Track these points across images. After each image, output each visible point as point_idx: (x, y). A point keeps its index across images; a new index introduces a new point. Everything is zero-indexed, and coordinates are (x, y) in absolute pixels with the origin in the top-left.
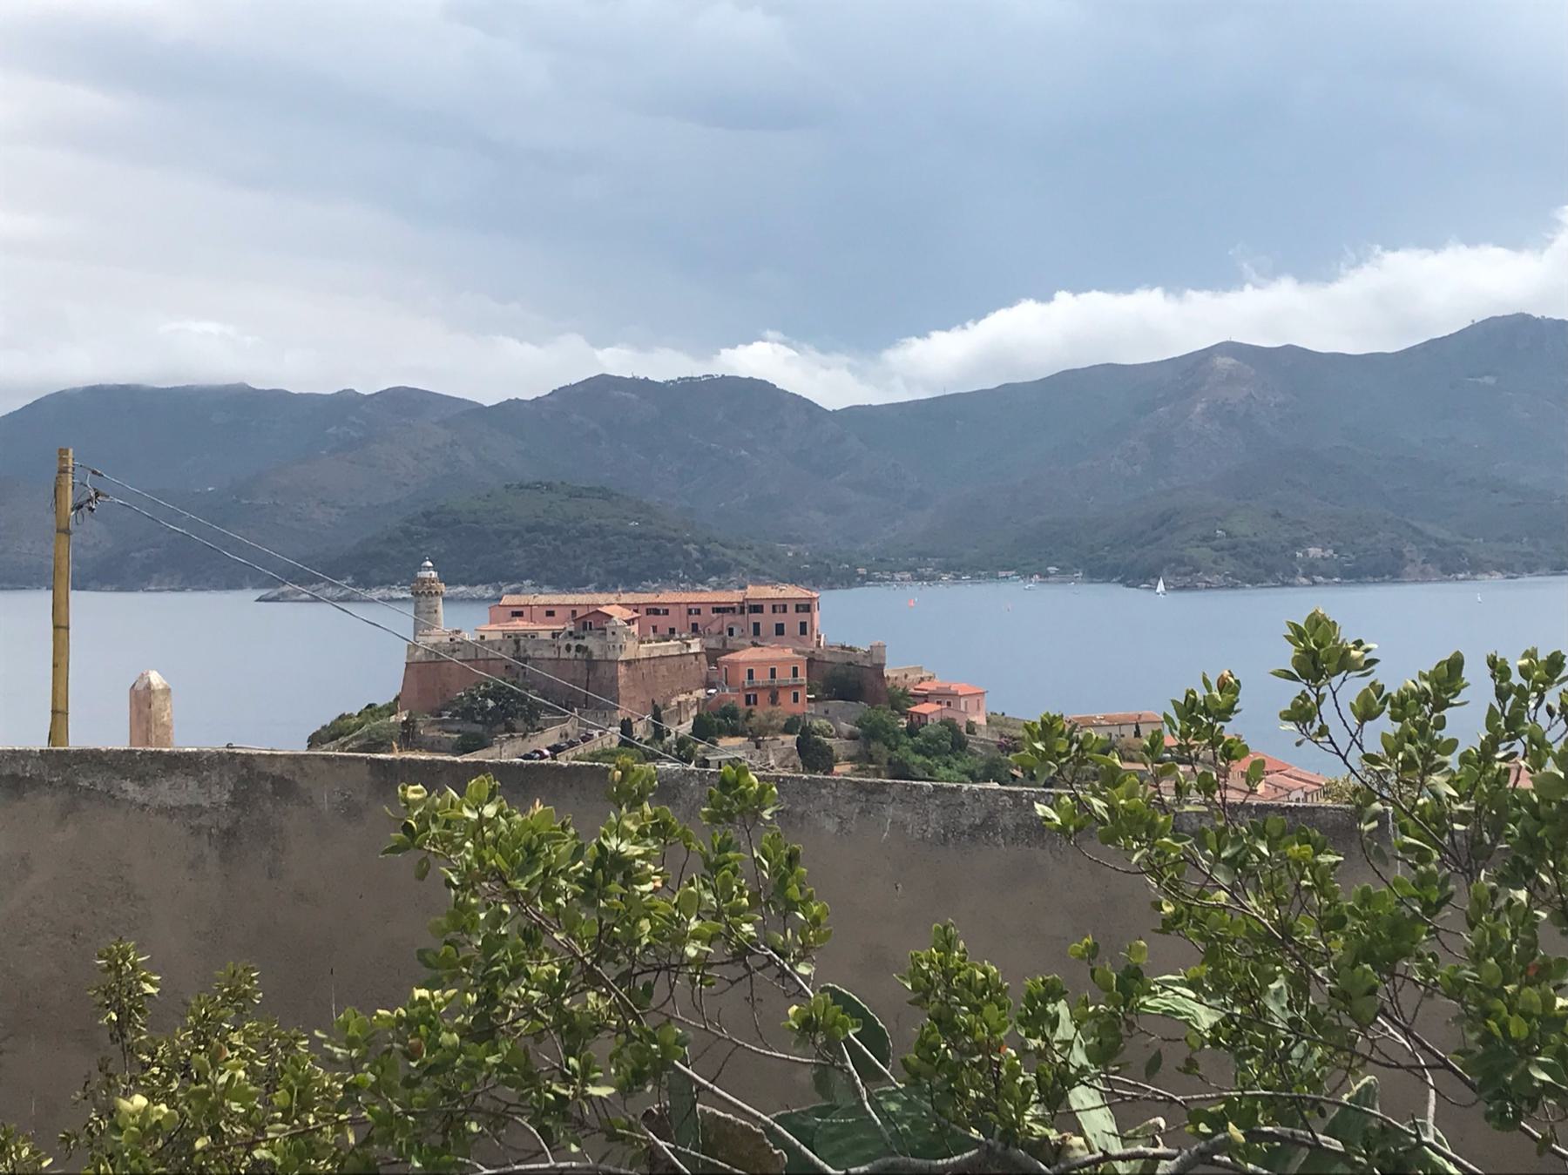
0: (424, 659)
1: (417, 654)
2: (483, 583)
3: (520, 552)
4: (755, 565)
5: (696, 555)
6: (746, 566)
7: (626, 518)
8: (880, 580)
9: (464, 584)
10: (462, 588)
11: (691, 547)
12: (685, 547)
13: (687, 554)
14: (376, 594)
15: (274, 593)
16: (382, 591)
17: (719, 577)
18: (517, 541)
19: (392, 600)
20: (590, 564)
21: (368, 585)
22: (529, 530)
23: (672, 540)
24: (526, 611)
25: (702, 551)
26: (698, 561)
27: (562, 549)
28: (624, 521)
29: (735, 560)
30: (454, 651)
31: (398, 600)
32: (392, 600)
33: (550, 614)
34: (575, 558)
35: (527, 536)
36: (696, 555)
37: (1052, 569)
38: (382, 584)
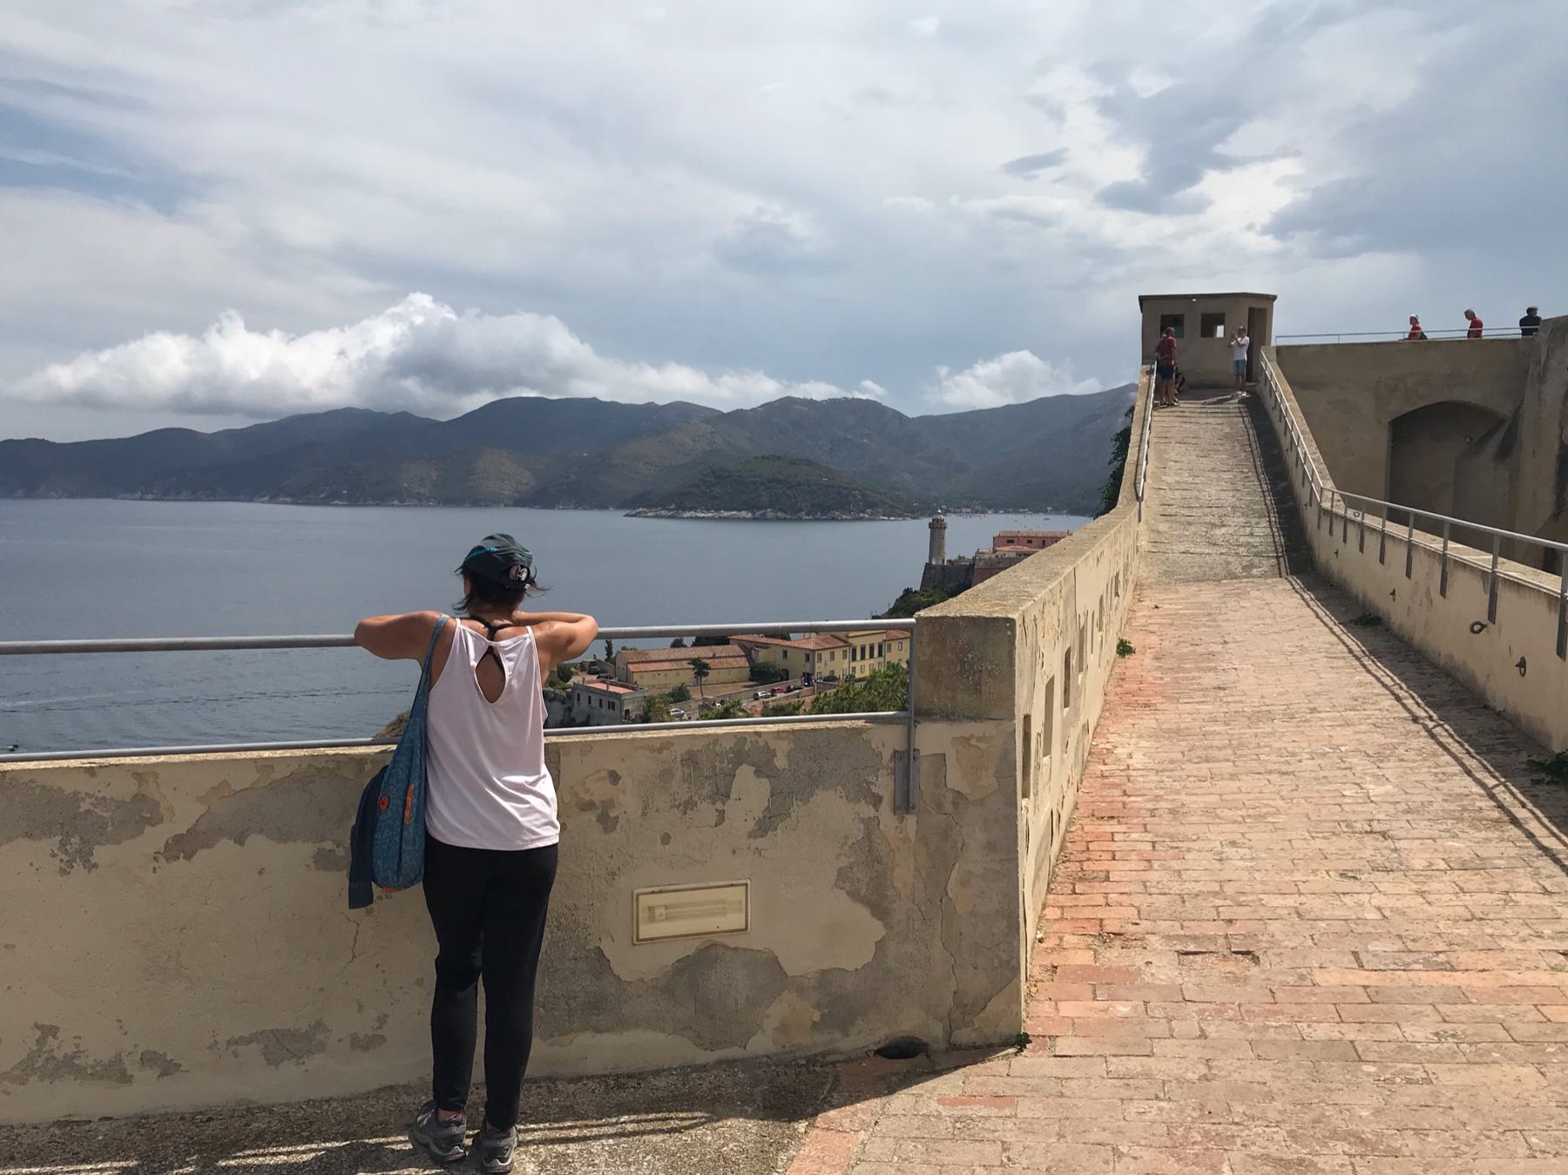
2: (745, 510)
3: (764, 493)
4: (890, 502)
5: (859, 497)
6: (886, 503)
8: (955, 513)
10: (734, 512)
11: (857, 492)
13: (855, 496)
14: (688, 514)
15: (634, 512)
16: (692, 512)
18: (763, 487)
19: (697, 518)
21: (684, 510)
22: (769, 482)
23: (846, 489)
24: (1016, 540)
25: (863, 495)
26: (860, 500)
27: (787, 492)
30: (999, 563)
32: (697, 518)
33: (1030, 542)
35: (768, 485)
36: (859, 497)
37: (1049, 508)
38: (690, 509)
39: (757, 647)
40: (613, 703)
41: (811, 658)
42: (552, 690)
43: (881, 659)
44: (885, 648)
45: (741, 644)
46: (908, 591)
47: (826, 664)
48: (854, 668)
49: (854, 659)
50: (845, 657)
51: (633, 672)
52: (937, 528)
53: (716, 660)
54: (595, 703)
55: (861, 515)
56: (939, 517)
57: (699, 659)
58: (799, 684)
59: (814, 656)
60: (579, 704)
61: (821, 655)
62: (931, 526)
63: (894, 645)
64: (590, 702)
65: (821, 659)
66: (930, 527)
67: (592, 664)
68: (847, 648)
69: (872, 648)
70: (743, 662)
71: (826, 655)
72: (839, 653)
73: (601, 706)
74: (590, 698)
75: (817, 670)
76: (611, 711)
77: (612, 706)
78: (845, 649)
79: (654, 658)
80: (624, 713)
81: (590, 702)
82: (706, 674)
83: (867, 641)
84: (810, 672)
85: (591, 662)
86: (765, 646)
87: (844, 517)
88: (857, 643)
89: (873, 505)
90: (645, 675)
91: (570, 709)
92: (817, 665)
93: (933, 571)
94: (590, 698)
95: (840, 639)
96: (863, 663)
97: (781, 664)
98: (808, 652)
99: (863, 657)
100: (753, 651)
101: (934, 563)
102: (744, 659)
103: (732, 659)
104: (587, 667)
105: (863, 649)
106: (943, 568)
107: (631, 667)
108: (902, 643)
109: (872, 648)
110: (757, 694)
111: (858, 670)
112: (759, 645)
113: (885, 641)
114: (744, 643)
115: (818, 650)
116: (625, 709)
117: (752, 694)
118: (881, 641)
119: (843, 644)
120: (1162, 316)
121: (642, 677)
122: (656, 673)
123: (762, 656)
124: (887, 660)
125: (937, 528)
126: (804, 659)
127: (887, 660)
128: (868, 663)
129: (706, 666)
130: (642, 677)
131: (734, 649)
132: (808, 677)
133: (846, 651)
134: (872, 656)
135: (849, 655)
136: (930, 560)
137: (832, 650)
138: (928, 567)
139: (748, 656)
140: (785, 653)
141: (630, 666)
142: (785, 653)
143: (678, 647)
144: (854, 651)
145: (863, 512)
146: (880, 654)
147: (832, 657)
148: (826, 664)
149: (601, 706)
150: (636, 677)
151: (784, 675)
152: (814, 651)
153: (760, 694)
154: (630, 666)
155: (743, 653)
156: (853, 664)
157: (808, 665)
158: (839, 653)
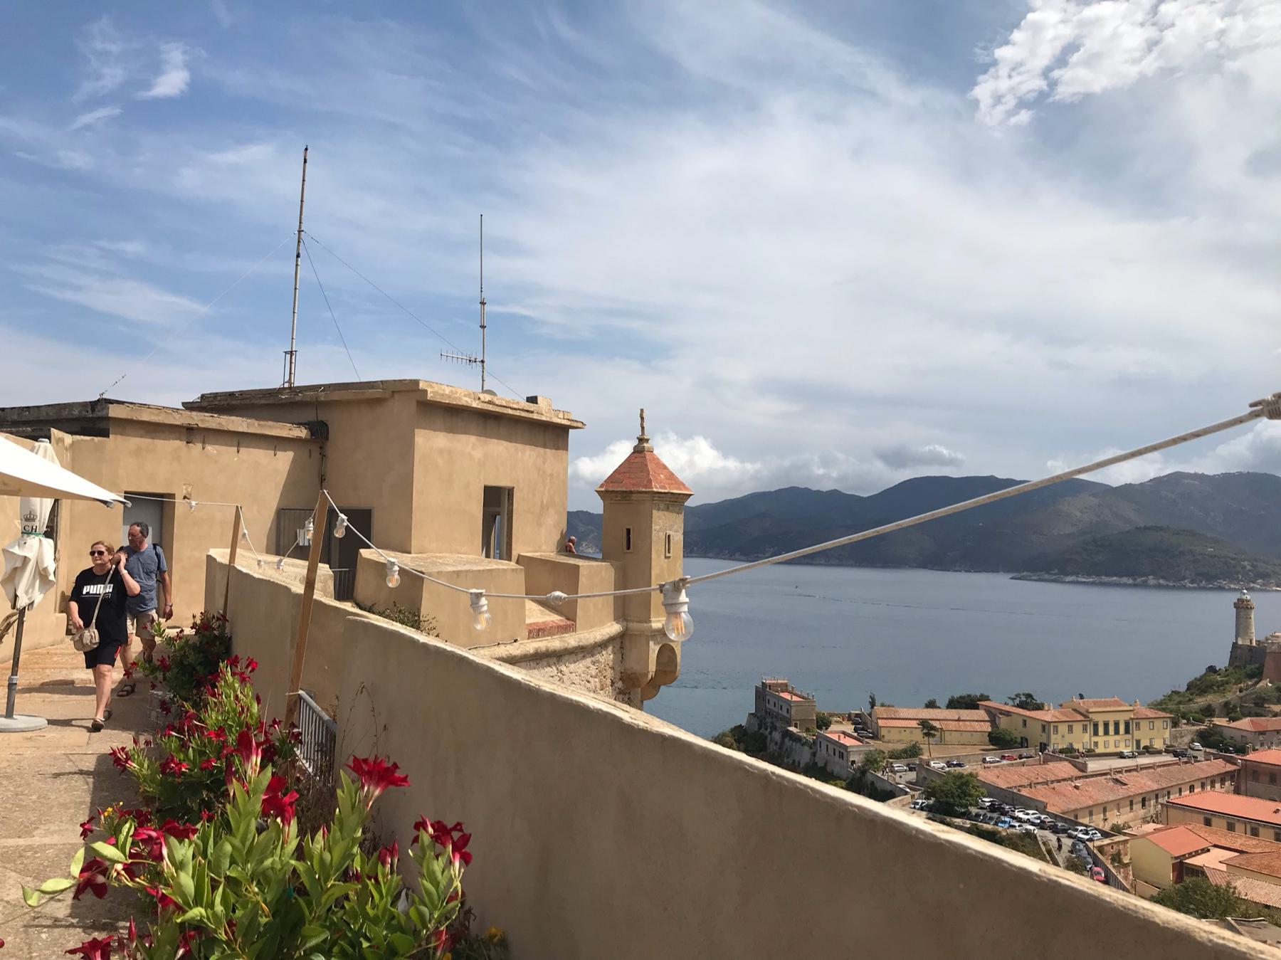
0: (1277, 651)
1: (1273, 647)
2: (1126, 576)
5: (1248, 567)
7: (1206, 546)
9: (1116, 575)
10: (1115, 578)
11: (1246, 563)
12: (1242, 563)
14: (1069, 579)
16: (1073, 577)
17: (1264, 580)
20: (1186, 569)
21: (1067, 575)
23: (1233, 559)
25: (1252, 566)
26: (1249, 570)
28: (1205, 548)
29: (1273, 571)
34: (1178, 566)
36: (1248, 567)
38: (1072, 574)
39: (1001, 714)
40: (843, 754)
41: (1046, 728)
42: (805, 735)
43: (1129, 736)
44: (1132, 726)
45: (989, 711)
46: (1212, 669)
47: (1063, 736)
48: (1096, 744)
49: (1096, 733)
51: (881, 727)
52: (1242, 608)
53: (961, 723)
54: (831, 752)
55: (1252, 585)
56: (1244, 597)
58: (1032, 752)
60: (821, 751)
61: (1057, 727)
62: (1236, 606)
63: (1144, 724)
64: (827, 750)
65: (1057, 731)
66: (1235, 607)
67: (857, 715)
68: (1088, 723)
69: (1117, 724)
70: (987, 727)
71: (1063, 728)
72: (1078, 728)
73: (834, 754)
74: (827, 746)
76: (841, 759)
77: (841, 756)
78: (1085, 723)
79: (902, 715)
80: (850, 764)
81: (827, 750)
82: (934, 736)
83: (1111, 718)
84: (1045, 741)
85: (857, 714)
86: (1008, 714)
87: (1232, 586)
88: (1100, 719)
89: (1264, 576)
90: (892, 730)
91: (814, 754)
92: (1053, 737)
93: (1239, 651)
94: (827, 746)
95: (1081, 714)
96: (1107, 738)
97: (1018, 734)
98: (1045, 723)
99: (1106, 733)
100: (997, 718)
101: (1240, 642)
102: (989, 724)
103: (977, 723)
104: (853, 717)
105: (1106, 725)
106: (1250, 648)
107: (881, 723)
108: (1153, 722)
109: (1117, 724)
110: (985, 759)
111: (1101, 745)
112: (1003, 712)
113: (1132, 719)
114: (993, 711)
115: (1053, 722)
116: (851, 759)
117: (981, 757)
118: (1127, 718)
119: (1082, 718)
121: (889, 732)
122: (903, 730)
123: (1003, 722)
124: (1135, 738)
125: (1242, 608)
126: (1040, 728)
127: (1135, 738)
128: (1112, 738)
129: (934, 728)
130: (889, 732)
131: (981, 714)
132: (1043, 747)
133: (1086, 725)
134: (1117, 732)
135: (1090, 729)
136: (1237, 639)
137: (1070, 724)
138: (1235, 645)
139: (993, 721)
140: (1025, 722)
141: (880, 721)
142: (1025, 722)
143: (932, 708)
144: (1096, 726)
145: (1254, 583)
146: (1127, 731)
147: (1070, 729)
148: (1063, 736)
149: (834, 754)
150: (883, 732)
151: (1024, 743)
152: (1049, 723)
153: (988, 759)
154: (880, 721)
155: (987, 718)
156: (1095, 739)
157: (1044, 735)
158: (1078, 728)
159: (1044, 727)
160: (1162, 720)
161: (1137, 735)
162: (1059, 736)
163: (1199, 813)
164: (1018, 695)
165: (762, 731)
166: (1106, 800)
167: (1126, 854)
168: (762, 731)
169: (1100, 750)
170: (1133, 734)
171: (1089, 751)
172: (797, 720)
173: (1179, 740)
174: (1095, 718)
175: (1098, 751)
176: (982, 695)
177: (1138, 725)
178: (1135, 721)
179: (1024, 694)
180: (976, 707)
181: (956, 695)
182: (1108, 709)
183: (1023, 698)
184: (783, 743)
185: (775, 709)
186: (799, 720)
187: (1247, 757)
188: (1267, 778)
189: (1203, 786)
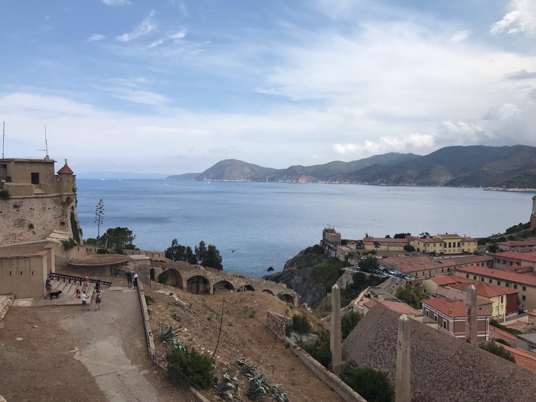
9: (533, 188)
10: (532, 189)
14: (511, 190)
15: (487, 189)
19: (515, 191)
21: (509, 188)
31: (516, 191)
32: (515, 191)
38: (512, 187)
43: (459, 248)
44: (461, 244)
47: (432, 248)
48: (445, 251)
49: (445, 247)
50: (441, 245)
57: (377, 242)
59: (426, 245)
61: (429, 244)
65: (429, 246)
68: (442, 243)
69: (454, 244)
75: (427, 250)
78: (441, 243)
84: (424, 250)
88: (447, 242)
90: (369, 246)
92: (427, 248)
96: (450, 248)
113: (461, 241)
120: (32, 174)
121: (368, 246)
127: (462, 248)
128: (452, 249)
133: (441, 244)
135: (443, 244)
137: (435, 243)
144: (445, 244)
146: (459, 246)
148: (432, 248)
152: (426, 243)
159: (424, 244)
160: (473, 242)
161: (463, 247)
162: (430, 248)
163: (465, 273)
164: (423, 233)
165: (324, 246)
166: (431, 268)
167: (422, 284)
168: (324, 246)
169: (447, 253)
170: (461, 248)
171: (441, 253)
172: (333, 242)
173: (481, 250)
174: (446, 241)
175: (445, 253)
176: (408, 233)
177: (463, 244)
178: (462, 242)
179: (425, 233)
180: (404, 238)
181: (398, 233)
182: (451, 238)
183: (425, 235)
184: (328, 250)
185: (328, 239)
186: (335, 242)
187: (496, 254)
188: (503, 262)
189: (483, 265)
